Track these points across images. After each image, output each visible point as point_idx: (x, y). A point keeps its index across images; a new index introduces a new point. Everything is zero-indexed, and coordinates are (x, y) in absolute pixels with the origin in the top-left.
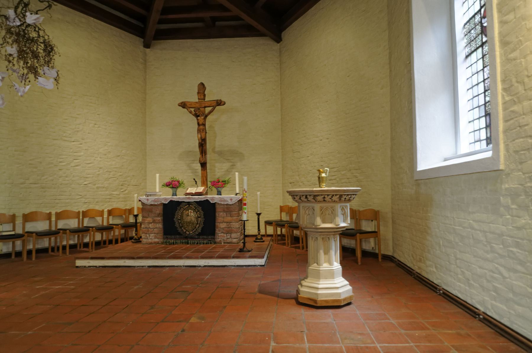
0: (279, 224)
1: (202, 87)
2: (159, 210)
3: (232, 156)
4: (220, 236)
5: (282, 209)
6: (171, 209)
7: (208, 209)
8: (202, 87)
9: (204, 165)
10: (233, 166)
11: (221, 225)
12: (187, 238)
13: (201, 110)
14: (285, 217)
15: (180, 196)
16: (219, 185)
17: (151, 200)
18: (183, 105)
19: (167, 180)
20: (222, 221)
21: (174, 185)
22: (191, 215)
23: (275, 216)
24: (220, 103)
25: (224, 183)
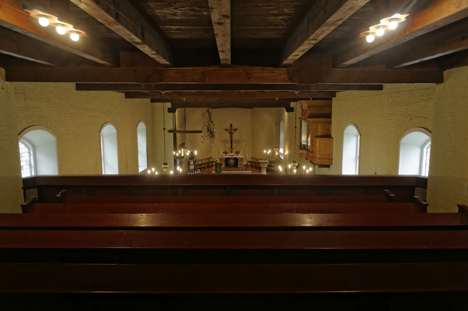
0: (252, 162)
1: (231, 125)
2: (224, 160)
3: (238, 142)
4: (239, 166)
5: (252, 158)
6: (227, 160)
7: (236, 160)
8: (231, 125)
9: (232, 147)
10: (237, 145)
11: (239, 163)
14: (253, 161)
15: (228, 156)
16: (237, 153)
17: (222, 157)
18: (226, 130)
21: (226, 153)
22: (232, 161)
23: (250, 160)
24: (236, 130)
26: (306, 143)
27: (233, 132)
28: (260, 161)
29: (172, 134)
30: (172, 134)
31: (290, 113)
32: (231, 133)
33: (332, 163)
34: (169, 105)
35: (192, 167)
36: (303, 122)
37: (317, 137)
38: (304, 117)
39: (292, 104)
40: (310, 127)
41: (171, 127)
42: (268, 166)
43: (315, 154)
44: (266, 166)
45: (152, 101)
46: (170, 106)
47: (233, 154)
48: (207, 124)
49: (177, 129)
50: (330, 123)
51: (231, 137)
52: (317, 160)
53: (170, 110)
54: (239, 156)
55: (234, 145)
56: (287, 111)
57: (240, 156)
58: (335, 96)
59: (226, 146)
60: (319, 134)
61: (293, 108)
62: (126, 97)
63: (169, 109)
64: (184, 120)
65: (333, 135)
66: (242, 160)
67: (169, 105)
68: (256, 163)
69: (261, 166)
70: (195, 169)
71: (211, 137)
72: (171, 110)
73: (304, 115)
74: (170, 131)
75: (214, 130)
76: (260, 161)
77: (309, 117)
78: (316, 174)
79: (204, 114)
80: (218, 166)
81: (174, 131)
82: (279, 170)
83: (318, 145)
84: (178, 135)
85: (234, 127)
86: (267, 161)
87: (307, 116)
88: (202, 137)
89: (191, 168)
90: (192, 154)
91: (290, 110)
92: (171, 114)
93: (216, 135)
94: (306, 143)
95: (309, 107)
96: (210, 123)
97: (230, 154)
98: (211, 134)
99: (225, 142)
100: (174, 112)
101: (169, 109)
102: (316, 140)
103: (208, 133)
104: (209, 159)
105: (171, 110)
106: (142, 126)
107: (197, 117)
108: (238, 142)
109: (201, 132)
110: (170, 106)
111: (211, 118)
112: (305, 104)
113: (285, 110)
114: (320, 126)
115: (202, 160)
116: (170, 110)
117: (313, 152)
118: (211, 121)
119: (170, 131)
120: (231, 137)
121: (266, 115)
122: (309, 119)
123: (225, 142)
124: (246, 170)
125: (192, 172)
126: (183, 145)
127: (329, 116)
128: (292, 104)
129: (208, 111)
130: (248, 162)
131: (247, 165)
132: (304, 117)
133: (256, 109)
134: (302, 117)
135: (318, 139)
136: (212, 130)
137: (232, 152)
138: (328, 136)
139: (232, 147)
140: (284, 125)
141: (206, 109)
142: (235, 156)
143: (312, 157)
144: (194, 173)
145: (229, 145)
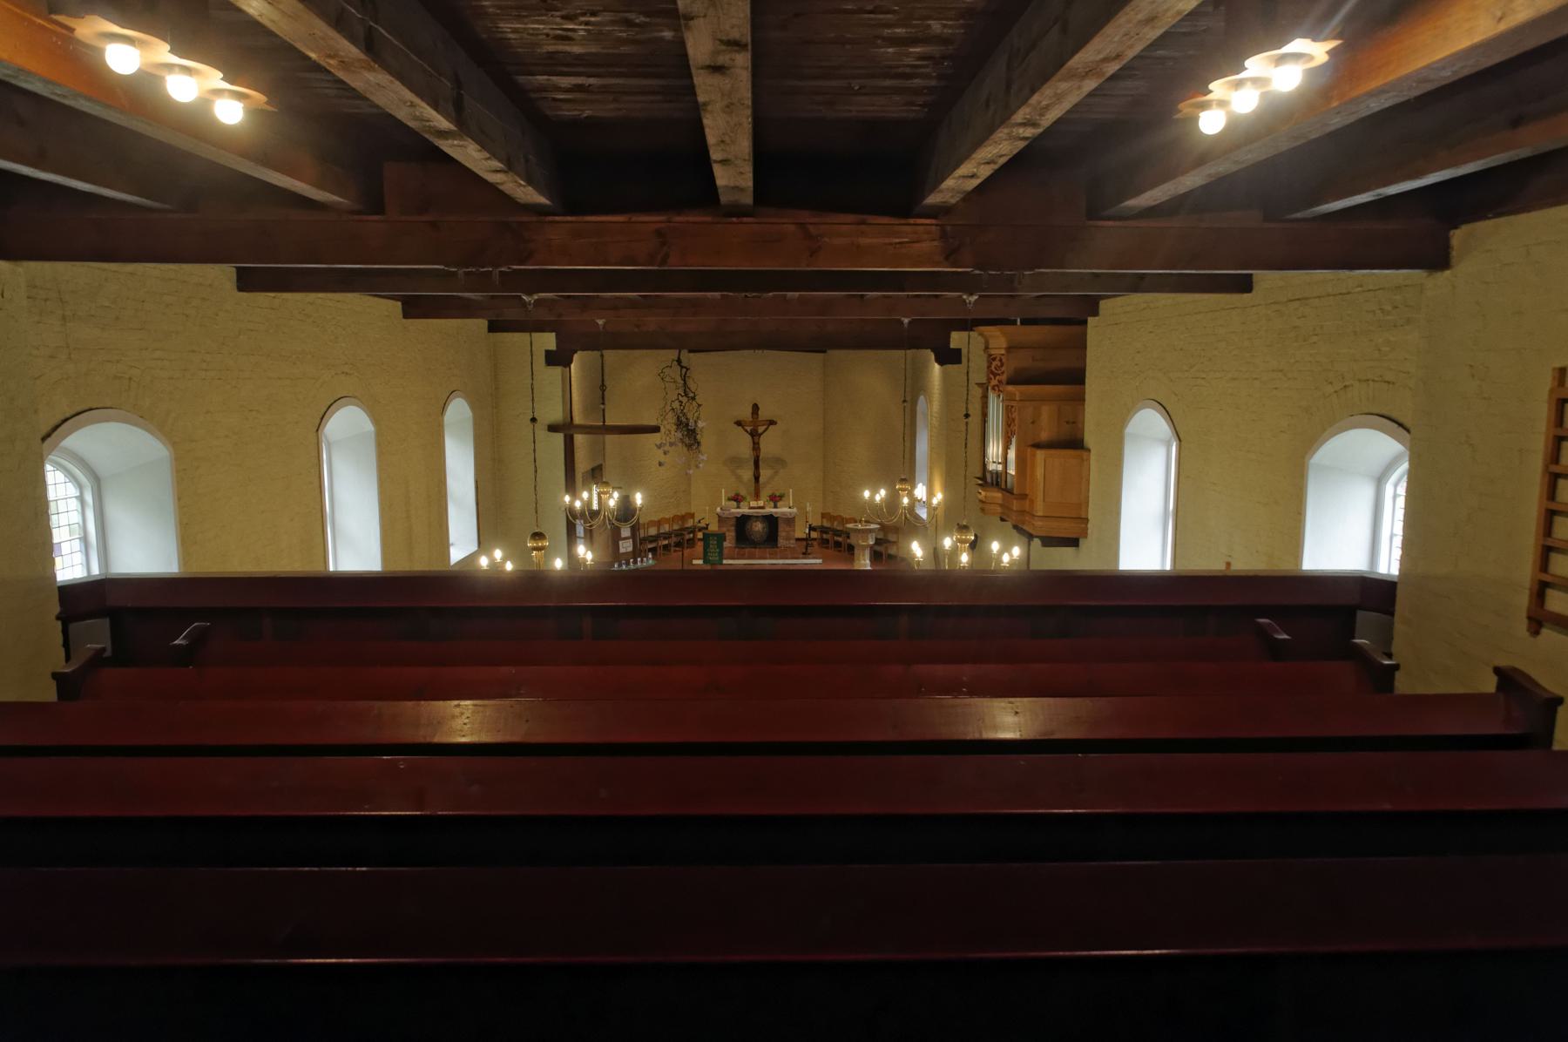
0: (823, 530)
1: (756, 408)
2: (733, 522)
3: (779, 462)
4: (781, 542)
5: (823, 516)
6: (742, 522)
7: (771, 521)
8: (756, 408)
9: (757, 478)
10: (776, 473)
11: (782, 533)
12: (754, 544)
13: (755, 426)
14: (826, 524)
15: (744, 510)
16: (775, 499)
18: (739, 423)
19: (732, 494)
20: (782, 531)
21: (737, 499)
22: (758, 527)
23: (816, 522)
24: (772, 423)
25: (781, 497)
26: (1000, 468)
27: (761, 429)
28: (850, 526)
29: (559, 438)
30: (559, 438)
31: (949, 366)
32: (754, 435)
33: (1085, 534)
34: (549, 341)
35: (626, 547)
36: (992, 396)
37: (1038, 446)
38: (994, 382)
39: (957, 339)
40: (1015, 415)
41: (556, 414)
42: (878, 542)
43: (1032, 502)
44: (871, 542)
45: (494, 327)
46: (553, 346)
47: (761, 503)
48: (676, 405)
49: (577, 420)
50: (1080, 399)
51: (756, 447)
52: (1039, 523)
53: (553, 359)
54: (783, 510)
55: (765, 473)
56: (941, 361)
57: (786, 510)
58: (1095, 313)
59: (739, 478)
60: (1044, 436)
61: (959, 351)
62: (405, 317)
63: (548, 353)
64: (600, 391)
65: (1089, 439)
66: (790, 521)
67: (549, 341)
68: (837, 533)
69: (853, 541)
70: (636, 553)
71: (689, 446)
72: (557, 359)
73: (995, 375)
74: (553, 428)
75: (700, 424)
76: (850, 526)
77: (1010, 382)
78: (1033, 567)
79: (667, 371)
80: (713, 542)
81: (565, 428)
82: (914, 556)
83: (1039, 472)
84: (579, 439)
85: (764, 414)
86: (873, 526)
87: (1004, 378)
88: (659, 447)
89: (622, 550)
90: (626, 502)
91: (949, 357)
92: (558, 370)
93: (706, 439)
94: (1000, 468)
95: (1009, 349)
96: (684, 400)
97: (753, 504)
98: (690, 436)
99: (734, 462)
100: (567, 363)
101: (548, 353)
102: (1034, 455)
103: (679, 435)
104: (683, 518)
105: (557, 359)
106: (458, 412)
107: (641, 381)
108: (779, 462)
109: (656, 429)
110: (553, 346)
111: (691, 383)
112: (998, 338)
113: (933, 356)
114: (1046, 412)
115: (659, 523)
116: (553, 359)
117: (1023, 497)
118: (687, 393)
119: (553, 428)
120: (756, 447)
121: (869, 376)
122: (1010, 388)
123: (734, 462)
124: (805, 554)
125: (628, 564)
126: (596, 475)
127: (1076, 377)
128: (957, 339)
129: (679, 361)
130: (812, 528)
131: (807, 540)
132: (994, 382)
133: (836, 355)
134: (989, 380)
135: (1040, 455)
136: (691, 423)
137: (757, 496)
138: (1073, 443)
139: (757, 478)
140: (931, 407)
141: (672, 354)
142: (770, 510)
143: (1022, 512)
144: (632, 566)
145: (747, 474)
